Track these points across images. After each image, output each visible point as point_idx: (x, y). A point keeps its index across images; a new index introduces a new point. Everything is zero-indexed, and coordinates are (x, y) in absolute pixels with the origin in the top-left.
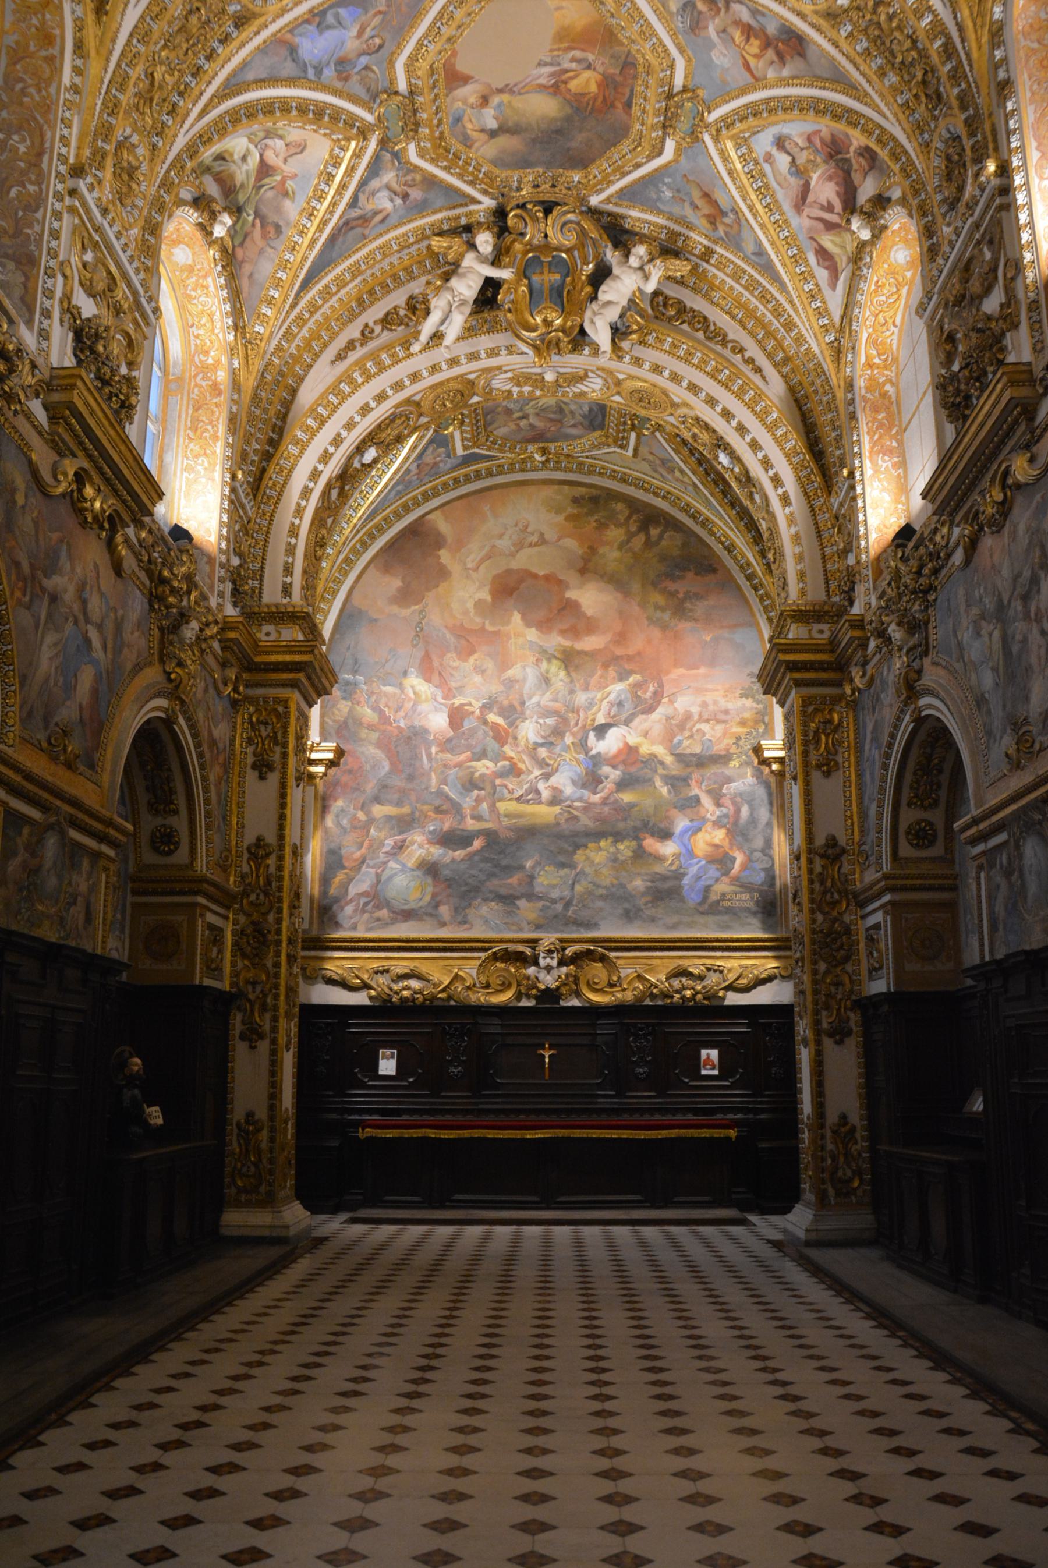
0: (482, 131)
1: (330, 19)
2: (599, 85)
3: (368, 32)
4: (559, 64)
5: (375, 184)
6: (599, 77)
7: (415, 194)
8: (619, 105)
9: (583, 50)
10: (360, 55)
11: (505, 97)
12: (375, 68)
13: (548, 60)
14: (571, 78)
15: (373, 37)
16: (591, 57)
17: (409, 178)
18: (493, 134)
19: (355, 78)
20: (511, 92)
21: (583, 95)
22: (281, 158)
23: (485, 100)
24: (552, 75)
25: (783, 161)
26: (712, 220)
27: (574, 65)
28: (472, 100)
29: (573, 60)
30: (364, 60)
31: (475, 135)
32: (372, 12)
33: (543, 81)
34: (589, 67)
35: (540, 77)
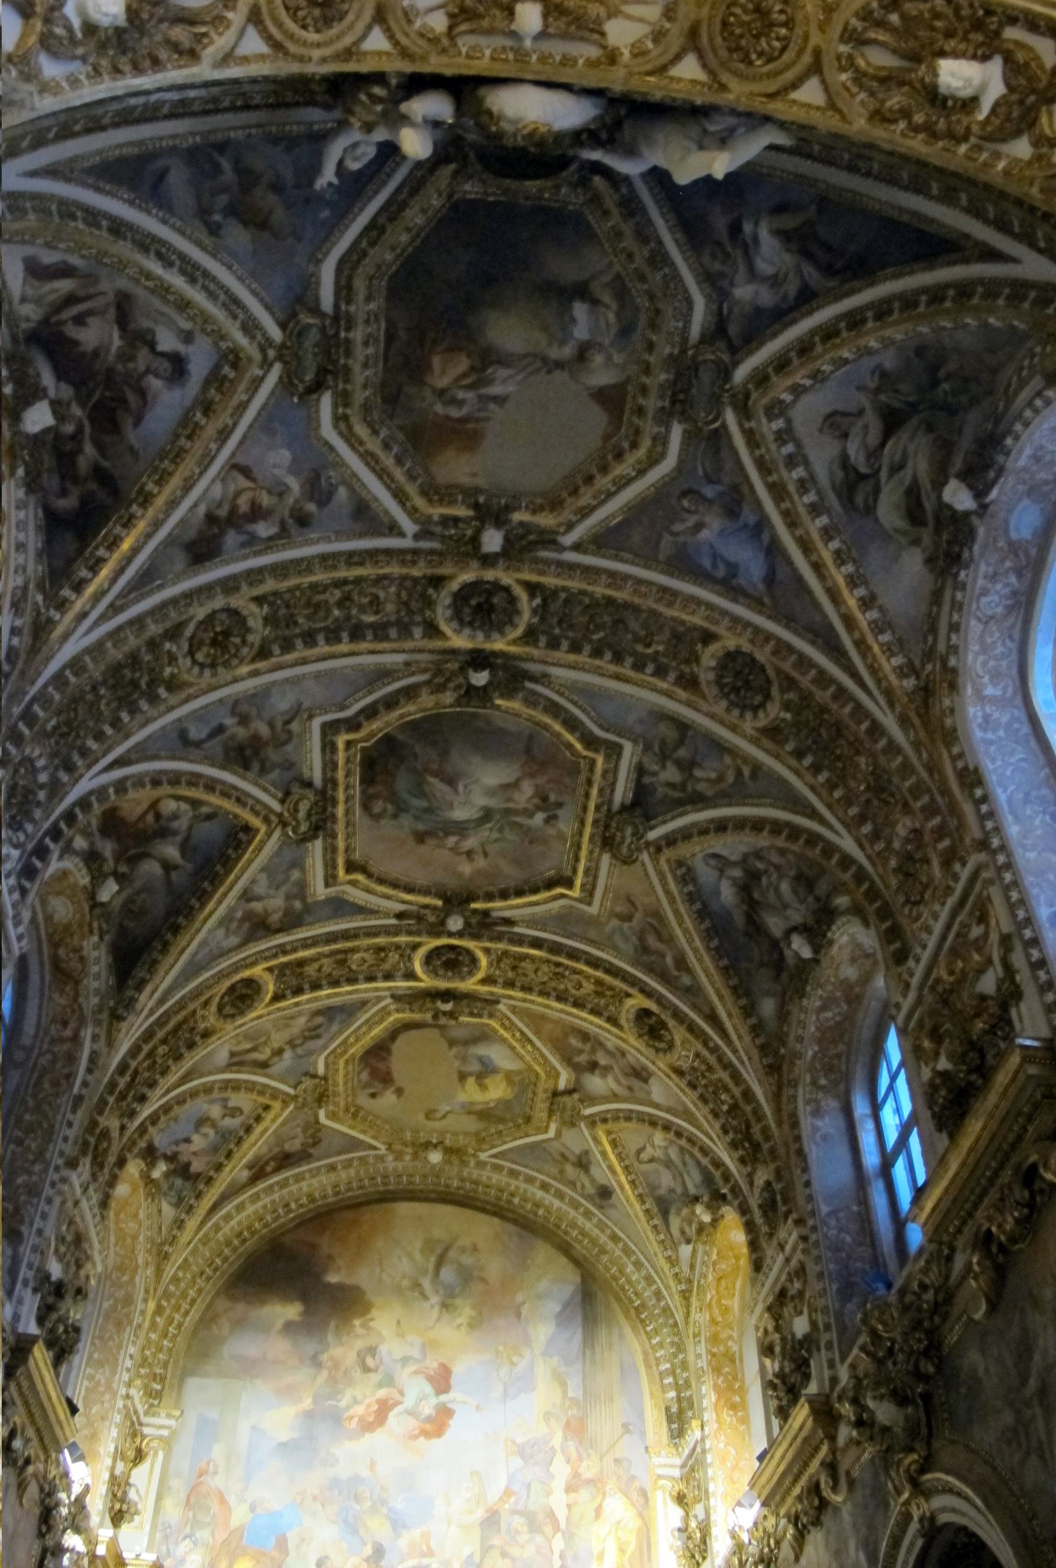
0: (595, 302)
1: (721, 572)
2: (429, 366)
3: (692, 520)
4: (480, 397)
5: (767, 298)
6: (429, 379)
7: (720, 223)
8: (402, 334)
9: (448, 418)
10: (709, 502)
11: (555, 353)
12: (700, 472)
13: (492, 406)
14: (464, 375)
15: (688, 511)
16: (439, 409)
17: (717, 266)
18: (582, 291)
19: (726, 479)
20: (545, 360)
21: (451, 350)
22: (860, 423)
23: (582, 354)
24: (489, 382)
25: (167, 342)
26: (247, 178)
27: (461, 395)
28: (598, 359)
29: (460, 403)
30: (709, 491)
31: (606, 298)
32: (681, 539)
33: (502, 373)
34: (441, 393)
35: (505, 381)
